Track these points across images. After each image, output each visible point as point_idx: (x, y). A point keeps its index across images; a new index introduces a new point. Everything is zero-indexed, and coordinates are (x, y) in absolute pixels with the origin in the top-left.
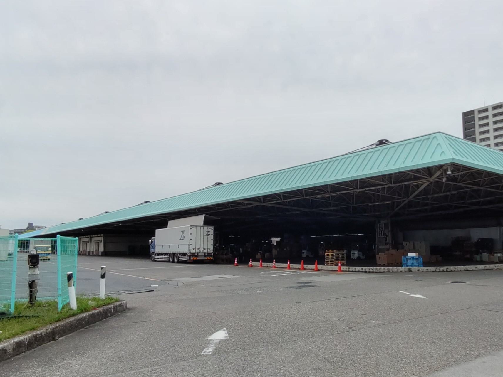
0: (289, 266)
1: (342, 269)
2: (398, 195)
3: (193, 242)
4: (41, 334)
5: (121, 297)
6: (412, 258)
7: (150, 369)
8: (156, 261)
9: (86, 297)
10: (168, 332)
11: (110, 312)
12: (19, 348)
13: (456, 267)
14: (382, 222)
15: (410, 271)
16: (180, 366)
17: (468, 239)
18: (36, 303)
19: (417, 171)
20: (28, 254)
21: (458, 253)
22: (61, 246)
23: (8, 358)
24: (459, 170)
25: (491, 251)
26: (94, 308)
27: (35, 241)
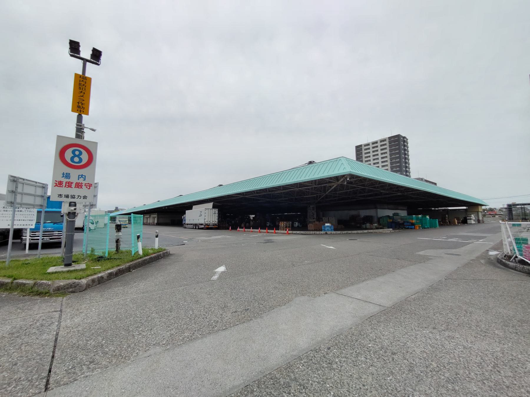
0: (260, 230)
1: (289, 233)
2: (320, 192)
3: (206, 218)
4: (123, 268)
5: (167, 248)
6: (328, 226)
7: (183, 288)
8: (186, 228)
9: (147, 248)
10: (193, 267)
11: (161, 256)
12: (111, 276)
13: (352, 231)
14: (311, 206)
15: (326, 233)
16: (199, 286)
17: (359, 216)
18: (120, 251)
19: (331, 178)
20: (115, 224)
21: (353, 224)
22: (134, 220)
23: (104, 282)
24: (353, 178)
25: (371, 223)
26: (152, 254)
27: (119, 217)
